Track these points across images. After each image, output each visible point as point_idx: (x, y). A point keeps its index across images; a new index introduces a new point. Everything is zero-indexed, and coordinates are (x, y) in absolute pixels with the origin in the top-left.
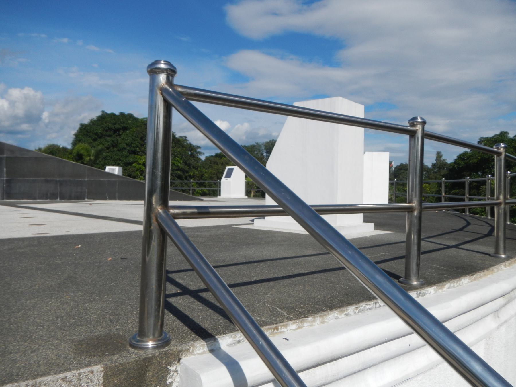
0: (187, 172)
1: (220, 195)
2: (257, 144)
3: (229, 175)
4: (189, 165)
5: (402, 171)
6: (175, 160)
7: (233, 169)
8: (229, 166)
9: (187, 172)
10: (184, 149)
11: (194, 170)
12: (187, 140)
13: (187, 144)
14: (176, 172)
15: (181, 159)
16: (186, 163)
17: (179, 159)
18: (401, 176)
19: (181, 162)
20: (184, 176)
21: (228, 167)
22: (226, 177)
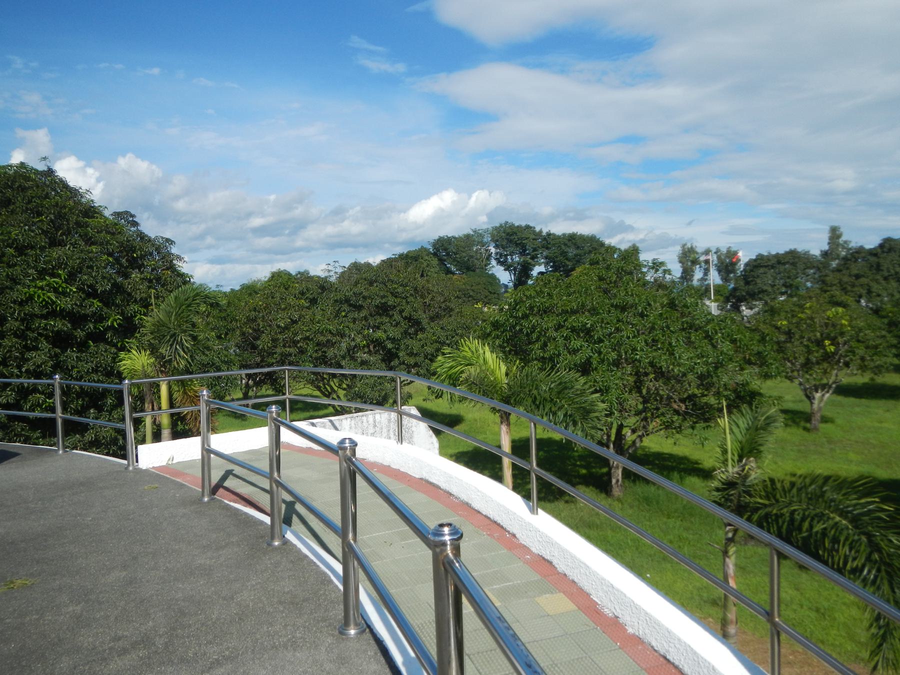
2: (475, 232)
5: (762, 270)
18: (758, 281)
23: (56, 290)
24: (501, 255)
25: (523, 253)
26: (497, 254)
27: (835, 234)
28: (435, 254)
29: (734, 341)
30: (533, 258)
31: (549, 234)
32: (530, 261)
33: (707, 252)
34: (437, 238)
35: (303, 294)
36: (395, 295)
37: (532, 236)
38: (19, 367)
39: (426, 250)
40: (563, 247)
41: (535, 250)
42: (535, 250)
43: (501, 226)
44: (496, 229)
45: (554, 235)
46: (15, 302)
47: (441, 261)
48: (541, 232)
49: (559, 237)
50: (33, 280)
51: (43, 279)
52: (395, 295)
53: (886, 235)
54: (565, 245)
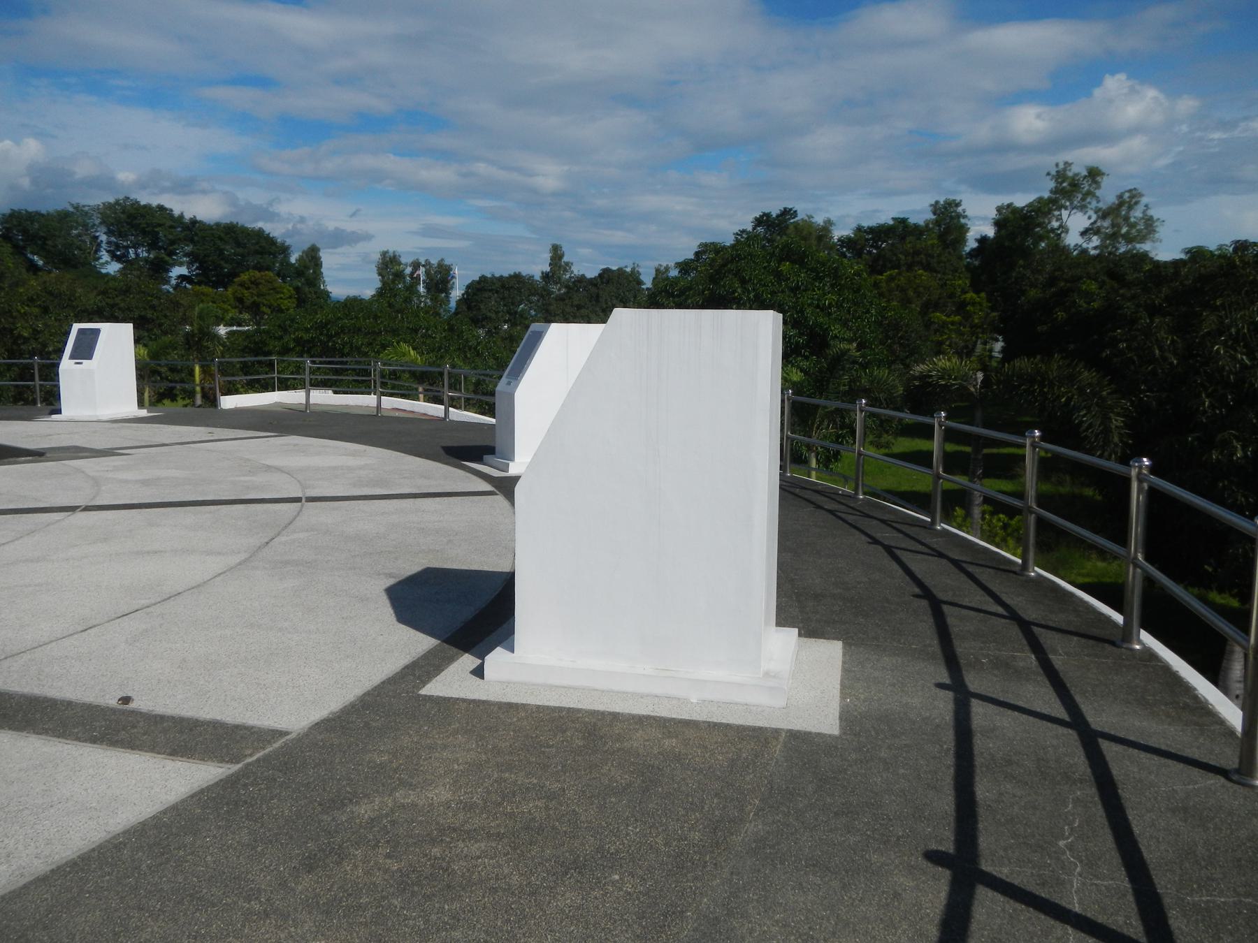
1: (59, 412)
2: (77, 208)
3: (85, 350)
5: (486, 295)
7: (97, 331)
8: (80, 322)
21: (76, 327)
22: (72, 357)
25: (153, 246)
26: (109, 243)
27: (557, 254)
29: (496, 359)
30: (171, 254)
31: (194, 222)
32: (167, 258)
33: (416, 265)
35: (31, 300)
36: (153, 308)
37: (169, 223)
40: (218, 242)
41: (173, 242)
42: (173, 242)
43: (117, 203)
44: (109, 206)
45: (200, 222)
47: (19, 250)
48: (181, 216)
52: (153, 308)
54: (220, 239)
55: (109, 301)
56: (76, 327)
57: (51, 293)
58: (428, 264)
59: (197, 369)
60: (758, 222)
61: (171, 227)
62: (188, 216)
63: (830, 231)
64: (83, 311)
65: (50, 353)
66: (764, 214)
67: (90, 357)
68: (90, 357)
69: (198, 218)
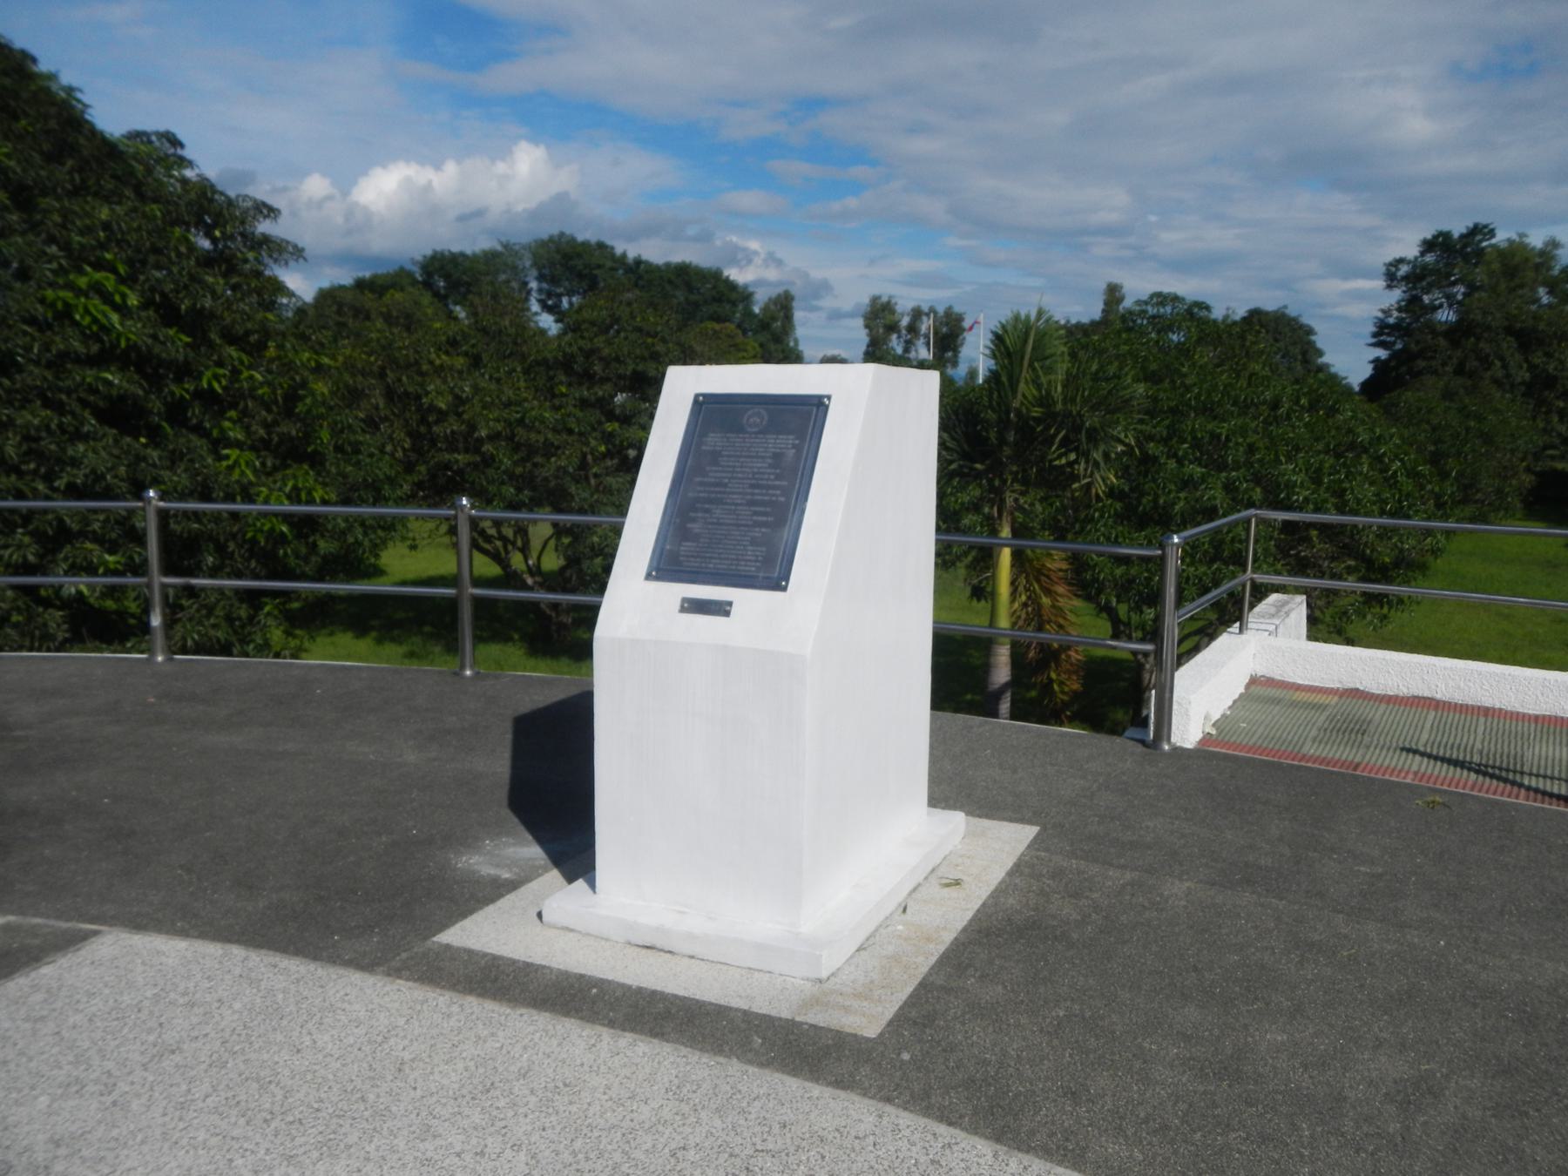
0: (184, 371)
2: (506, 246)
4: (196, 324)
6: (79, 292)
7: (807, 414)
9: (184, 371)
10: (156, 210)
11: (232, 351)
12: (183, 162)
13: (185, 181)
14: (90, 375)
15: (129, 280)
16: (168, 313)
17: (110, 282)
19: (133, 300)
20: (156, 405)
22: (666, 567)
23: (107, 298)
24: (550, 295)
26: (540, 290)
27: (1113, 294)
28: (428, 284)
31: (638, 262)
33: (917, 314)
34: (429, 252)
35: (453, 343)
37: (609, 264)
38: (49, 478)
39: (410, 274)
40: (668, 288)
43: (551, 239)
44: (543, 244)
45: (647, 263)
46: (32, 321)
48: (624, 255)
49: (658, 268)
50: (61, 271)
51: (81, 272)
53: (1252, 306)
54: (670, 282)
55: (581, 343)
56: (684, 385)
57: (484, 331)
58: (932, 310)
59: (1006, 555)
60: (1428, 246)
61: (612, 269)
62: (631, 255)
63: (1553, 258)
64: (538, 363)
65: (480, 441)
66: (1441, 234)
67: (772, 572)
68: (772, 572)
69: (644, 257)
